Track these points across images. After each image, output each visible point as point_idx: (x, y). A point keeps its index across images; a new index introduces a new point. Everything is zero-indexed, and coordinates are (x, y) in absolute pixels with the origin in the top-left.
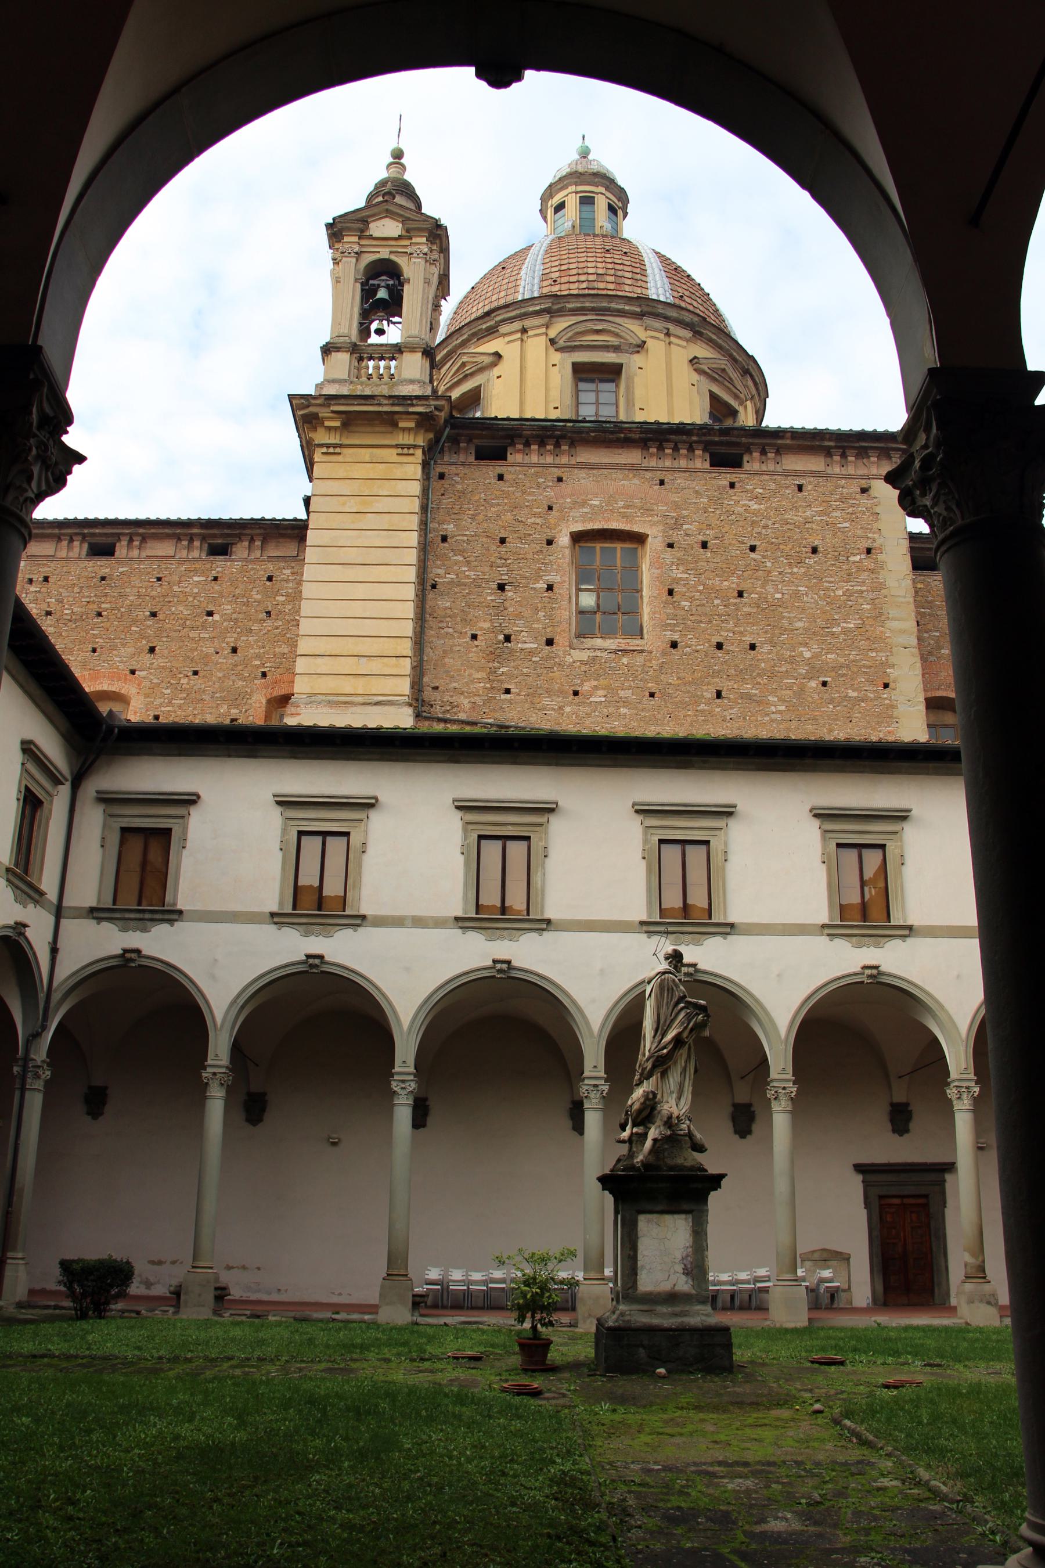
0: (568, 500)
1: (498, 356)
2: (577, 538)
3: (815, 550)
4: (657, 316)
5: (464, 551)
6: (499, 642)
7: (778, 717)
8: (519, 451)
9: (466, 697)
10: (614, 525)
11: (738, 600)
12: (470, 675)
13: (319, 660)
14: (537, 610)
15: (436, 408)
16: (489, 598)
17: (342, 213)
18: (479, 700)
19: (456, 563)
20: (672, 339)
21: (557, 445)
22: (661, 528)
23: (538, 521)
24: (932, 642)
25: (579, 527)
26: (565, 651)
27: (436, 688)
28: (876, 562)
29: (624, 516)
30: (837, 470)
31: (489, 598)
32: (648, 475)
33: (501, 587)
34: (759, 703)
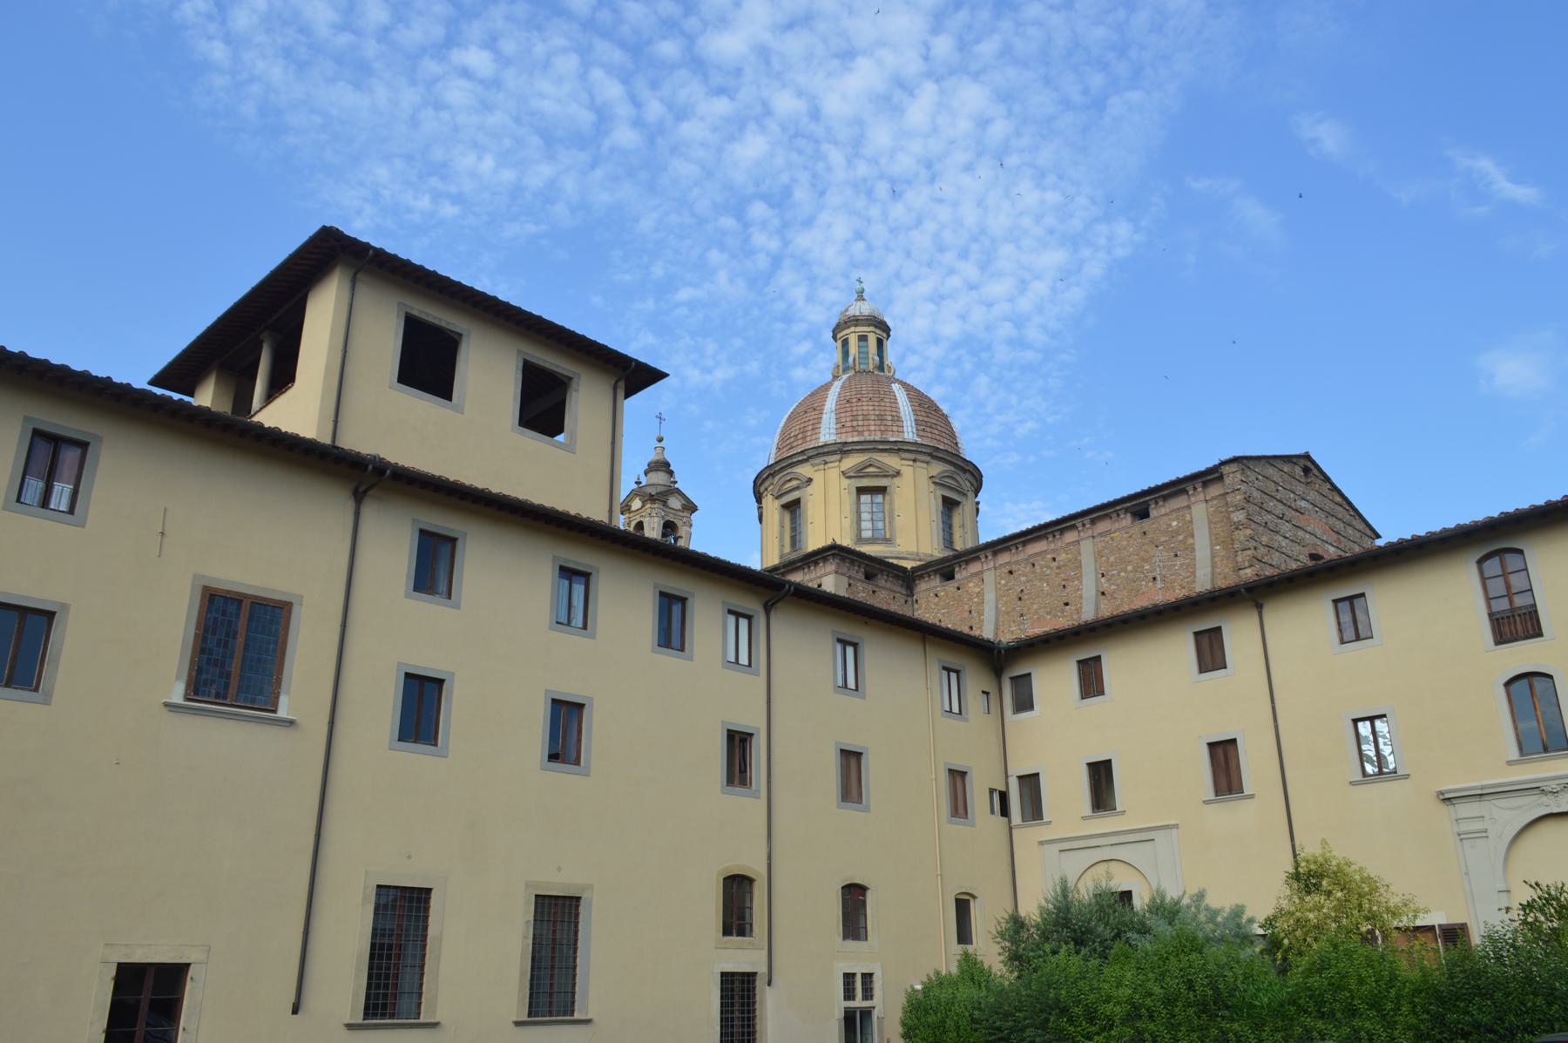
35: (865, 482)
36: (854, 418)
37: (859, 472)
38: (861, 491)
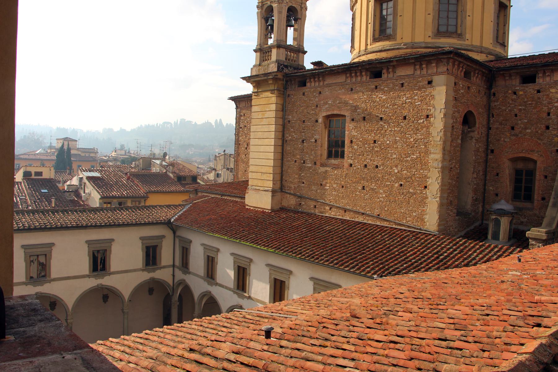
2: (328, 117)
3: (405, 118)
5: (294, 127)
10: (335, 112)
13: (254, 174)
15: (275, 75)
18: (296, 186)
21: (319, 78)
23: (313, 112)
24: (522, 126)
25: (325, 114)
28: (430, 123)
29: (338, 107)
34: (376, 193)
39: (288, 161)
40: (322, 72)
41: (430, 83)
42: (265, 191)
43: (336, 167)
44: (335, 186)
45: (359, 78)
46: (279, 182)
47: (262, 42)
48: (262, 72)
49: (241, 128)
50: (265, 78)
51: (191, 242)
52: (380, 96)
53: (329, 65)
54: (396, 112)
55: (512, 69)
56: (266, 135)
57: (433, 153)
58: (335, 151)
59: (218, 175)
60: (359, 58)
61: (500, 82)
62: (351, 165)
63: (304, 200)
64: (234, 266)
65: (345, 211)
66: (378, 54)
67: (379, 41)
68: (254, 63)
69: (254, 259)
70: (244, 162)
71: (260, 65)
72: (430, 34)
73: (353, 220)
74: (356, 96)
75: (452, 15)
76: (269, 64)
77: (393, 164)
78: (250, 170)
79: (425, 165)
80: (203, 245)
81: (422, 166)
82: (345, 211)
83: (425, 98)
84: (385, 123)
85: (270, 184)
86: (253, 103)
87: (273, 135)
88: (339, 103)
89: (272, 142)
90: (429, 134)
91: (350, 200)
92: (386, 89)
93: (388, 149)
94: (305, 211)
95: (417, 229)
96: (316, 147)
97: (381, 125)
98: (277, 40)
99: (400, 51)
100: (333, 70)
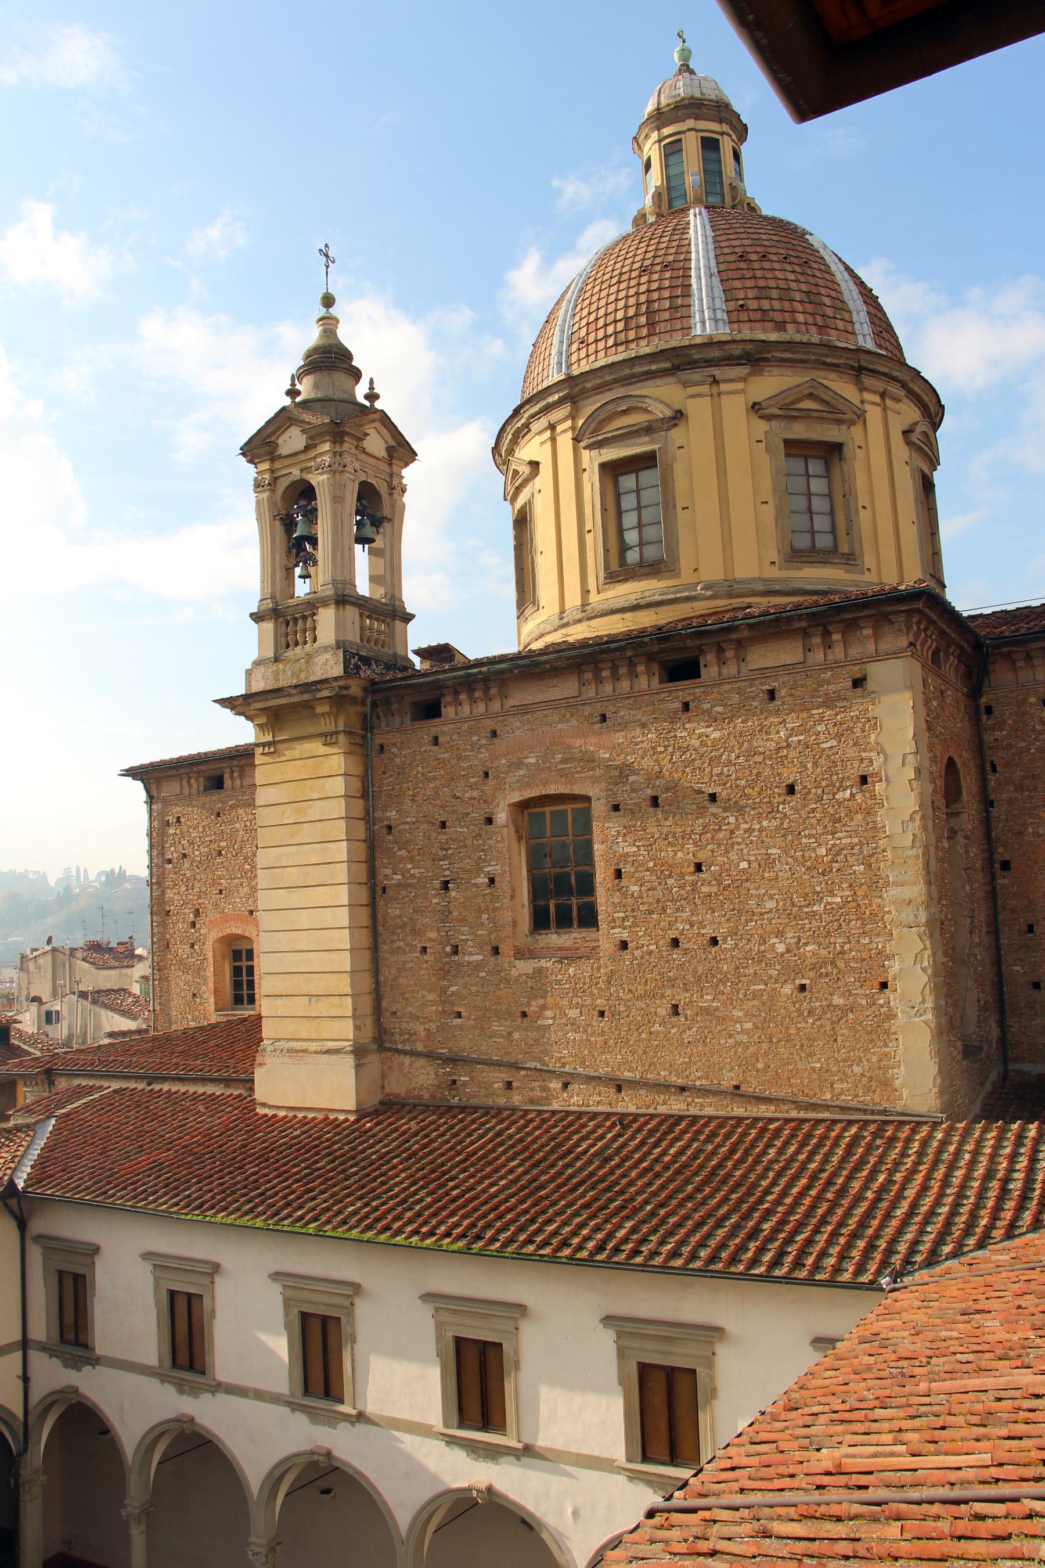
0: (504, 762)
1: (535, 465)
2: (523, 806)
3: (791, 790)
4: (693, 365)
6: (448, 955)
7: (745, 1038)
8: (450, 704)
9: (421, 1024)
10: (553, 789)
11: (694, 878)
12: (423, 997)
13: (279, 1002)
14: (480, 911)
15: (341, 688)
16: (434, 901)
17: (246, 439)
18: (432, 1026)
19: (402, 859)
20: (724, 387)
21: (487, 689)
22: (603, 785)
23: (475, 794)
25: (516, 797)
26: (510, 963)
27: (395, 1013)
28: (873, 797)
29: (562, 774)
30: (818, 656)
31: (434, 901)
32: (587, 710)
33: (445, 886)
34: (721, 1020)
35: (799, 431)
36: (763, 293)
37: (784, 410)
38: (794, 448)
39: (399, 951)
40: (502, 672)
41: (858, 683)
42: (328, 1052)
43: (569, 956)
44: (573, 1013)
45: (625, 685)
46: (369, 1021)
47: (278, 588)
48: (286, 680)
49: (170, 861)
50: (306, 697)
51: (97, 1250)
52: (700, 733)
53: (472, 657)
54: (759, 774)
55: (1031, 641)
56: (315, 875)
57: (896, 884)
58: (557, 907)
59: (50, 1017)
60: (564, 631)
61: (1002, 676)
62: (624, 945)
63: (467, 1069)
64: (287, 1314)
65: (619, 1089)
66: (628, 616)
67: (626, 580)
68: (254, 656)
69: (363, 1284)
70: (185, 968)
71: (277, 659)
72: (774, 556)
73: (651, 1111)
74: (619, 738)
75: (819, 504)
76: (309, 657)
77: (769, 929)
78: (264, 992)
79: (873, 921)
80: (147, 1256)
81: (863, 925)
82: (619, 1089)
83: (851, 730)
84: (725, 809)
85: (346, 1030)
86: (261, 775)
87: (341, 873)
88: (564, 761)
89: (343, 895)
90: (876, 829)
91: (633, 1053)
92: (719, 709)
93: (747, 885)
94: (473, 1102)
95: (873, 1112)
96: (495, 898)
97: (715, 815)
98: (334, 582)
99: (696, 605)
100: (536, 664)
